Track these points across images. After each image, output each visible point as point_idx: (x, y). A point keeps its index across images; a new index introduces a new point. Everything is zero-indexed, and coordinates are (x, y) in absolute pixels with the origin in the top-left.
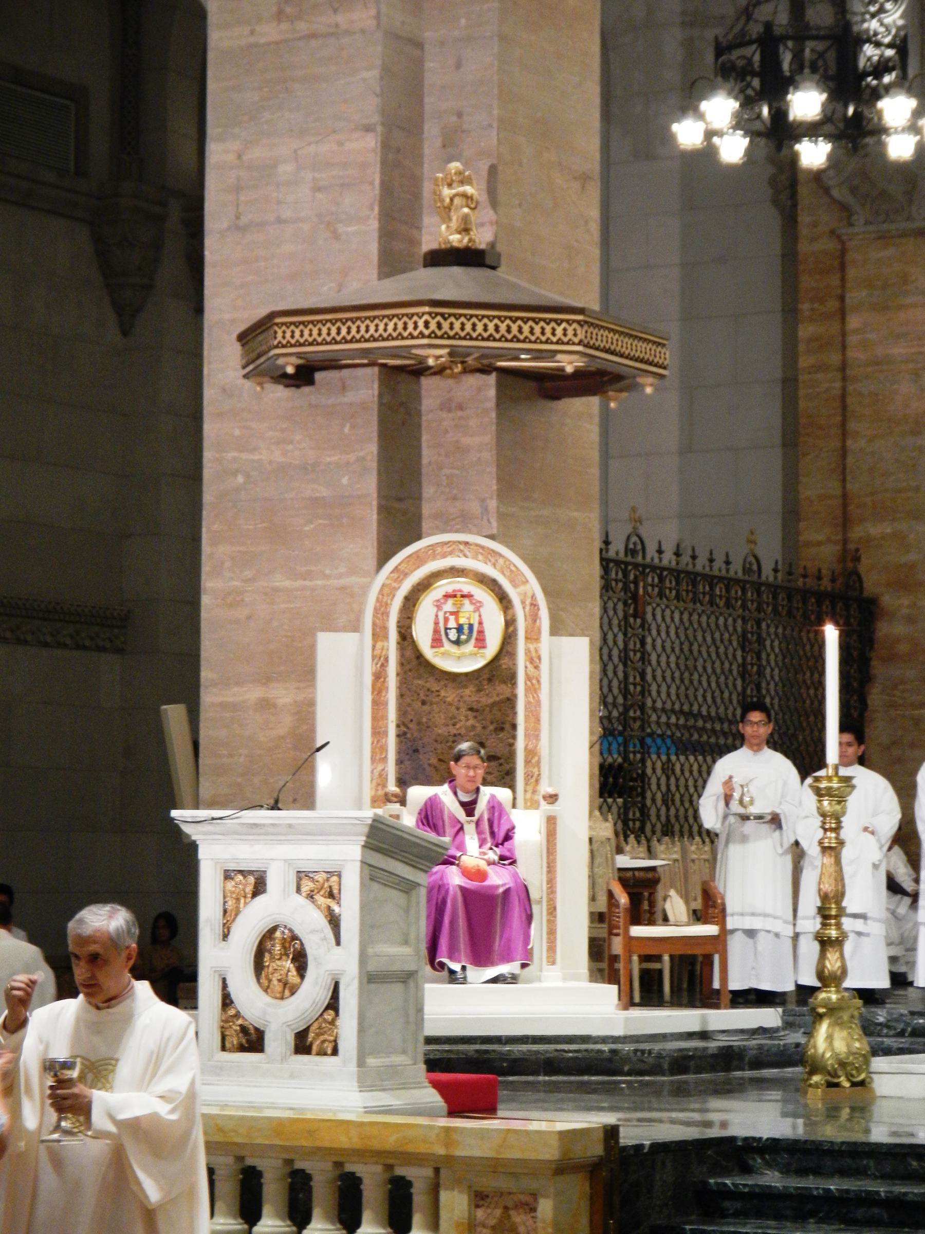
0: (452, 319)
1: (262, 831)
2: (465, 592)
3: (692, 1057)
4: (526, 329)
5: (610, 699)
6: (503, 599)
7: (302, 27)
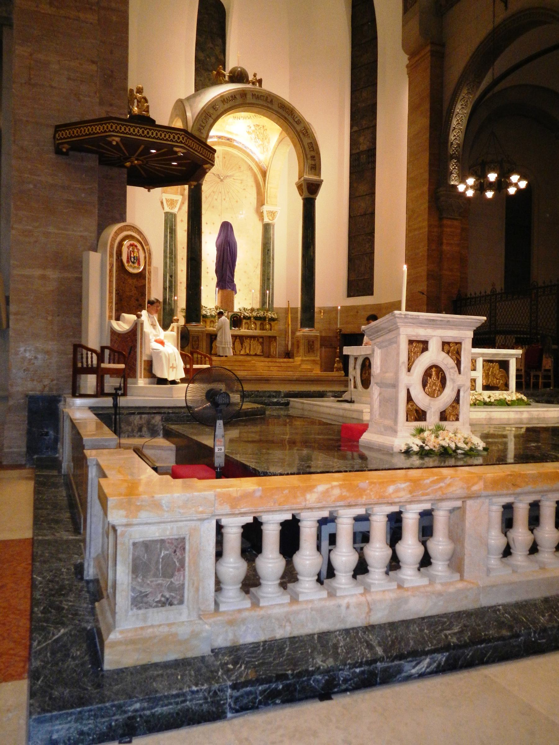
1: (434, 323)
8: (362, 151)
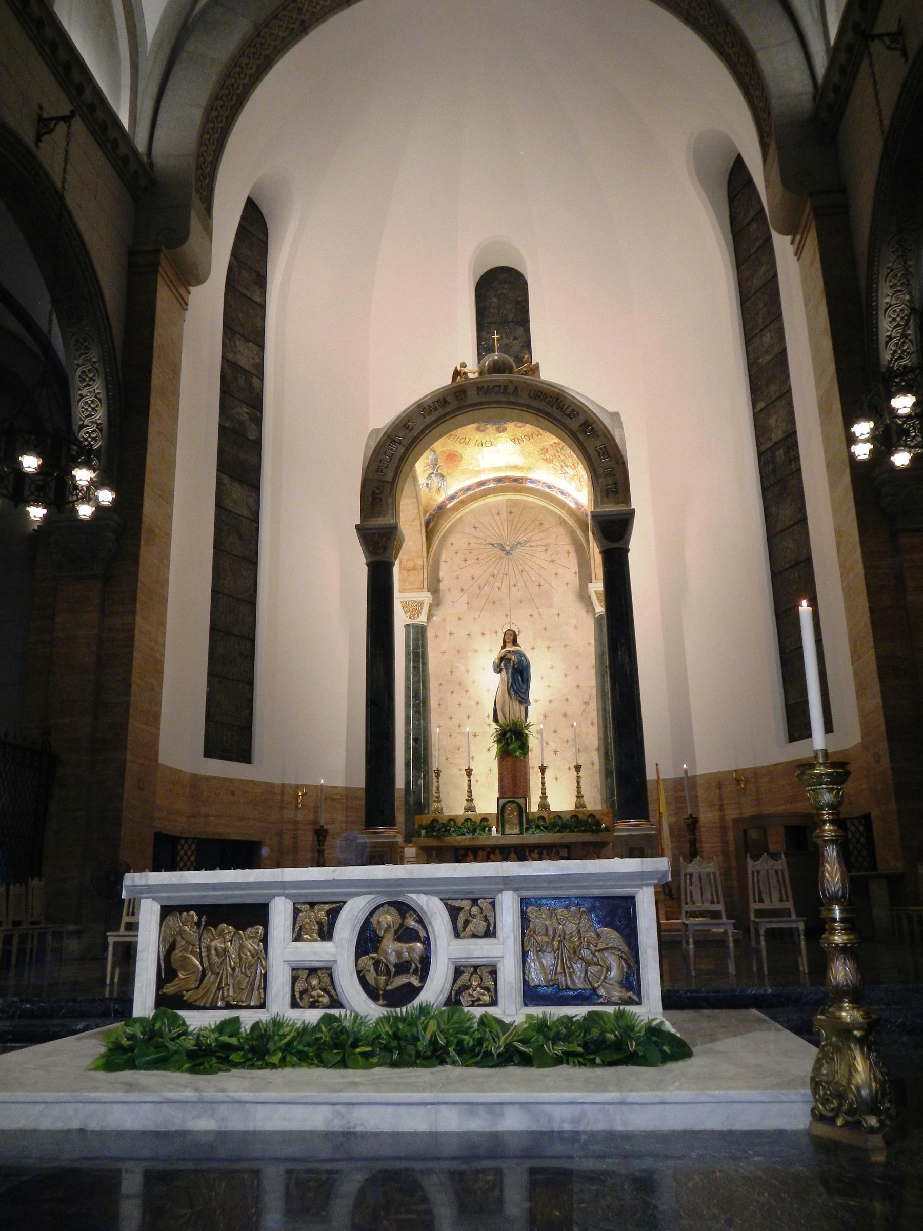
8: (776, 443)
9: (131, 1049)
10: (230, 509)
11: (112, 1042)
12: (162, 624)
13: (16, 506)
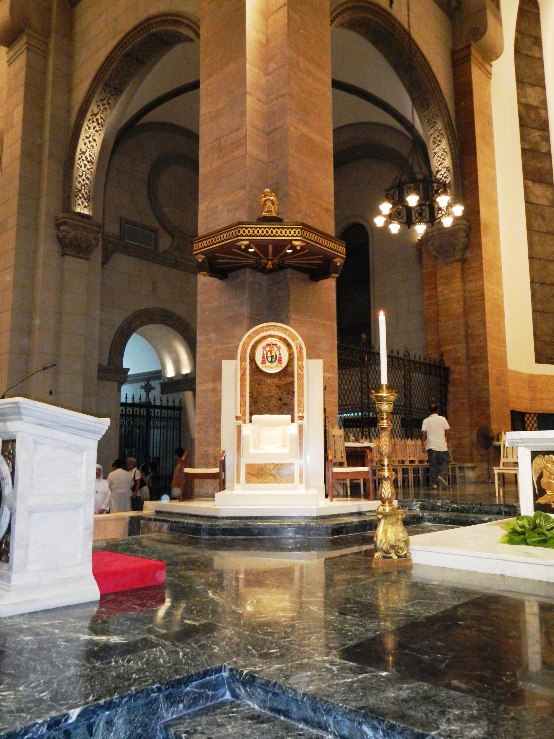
0: (249, 229)
2: (274, 343)
3: (344, 527)
4: (279, 232)
5: (342, 386)
6: (289, 346)
7: (225, 159)
9: (523, 533)
10: (535, 202)
11: (512, 529)
12: (499, 283)
13: (409, 227)
